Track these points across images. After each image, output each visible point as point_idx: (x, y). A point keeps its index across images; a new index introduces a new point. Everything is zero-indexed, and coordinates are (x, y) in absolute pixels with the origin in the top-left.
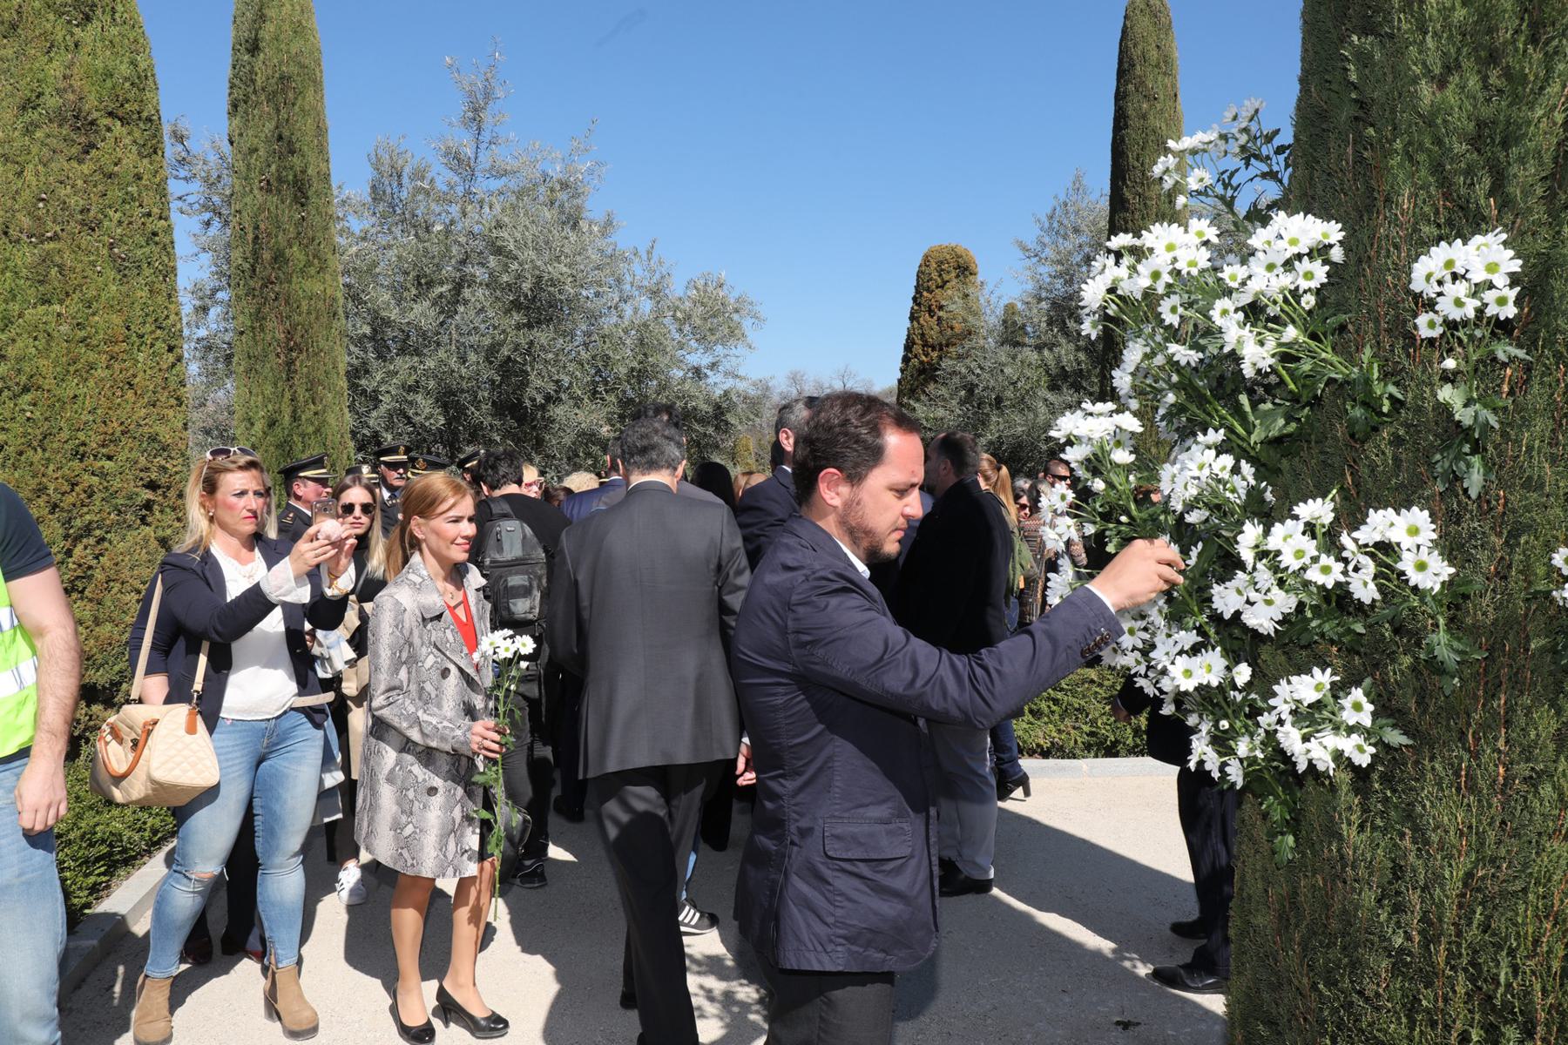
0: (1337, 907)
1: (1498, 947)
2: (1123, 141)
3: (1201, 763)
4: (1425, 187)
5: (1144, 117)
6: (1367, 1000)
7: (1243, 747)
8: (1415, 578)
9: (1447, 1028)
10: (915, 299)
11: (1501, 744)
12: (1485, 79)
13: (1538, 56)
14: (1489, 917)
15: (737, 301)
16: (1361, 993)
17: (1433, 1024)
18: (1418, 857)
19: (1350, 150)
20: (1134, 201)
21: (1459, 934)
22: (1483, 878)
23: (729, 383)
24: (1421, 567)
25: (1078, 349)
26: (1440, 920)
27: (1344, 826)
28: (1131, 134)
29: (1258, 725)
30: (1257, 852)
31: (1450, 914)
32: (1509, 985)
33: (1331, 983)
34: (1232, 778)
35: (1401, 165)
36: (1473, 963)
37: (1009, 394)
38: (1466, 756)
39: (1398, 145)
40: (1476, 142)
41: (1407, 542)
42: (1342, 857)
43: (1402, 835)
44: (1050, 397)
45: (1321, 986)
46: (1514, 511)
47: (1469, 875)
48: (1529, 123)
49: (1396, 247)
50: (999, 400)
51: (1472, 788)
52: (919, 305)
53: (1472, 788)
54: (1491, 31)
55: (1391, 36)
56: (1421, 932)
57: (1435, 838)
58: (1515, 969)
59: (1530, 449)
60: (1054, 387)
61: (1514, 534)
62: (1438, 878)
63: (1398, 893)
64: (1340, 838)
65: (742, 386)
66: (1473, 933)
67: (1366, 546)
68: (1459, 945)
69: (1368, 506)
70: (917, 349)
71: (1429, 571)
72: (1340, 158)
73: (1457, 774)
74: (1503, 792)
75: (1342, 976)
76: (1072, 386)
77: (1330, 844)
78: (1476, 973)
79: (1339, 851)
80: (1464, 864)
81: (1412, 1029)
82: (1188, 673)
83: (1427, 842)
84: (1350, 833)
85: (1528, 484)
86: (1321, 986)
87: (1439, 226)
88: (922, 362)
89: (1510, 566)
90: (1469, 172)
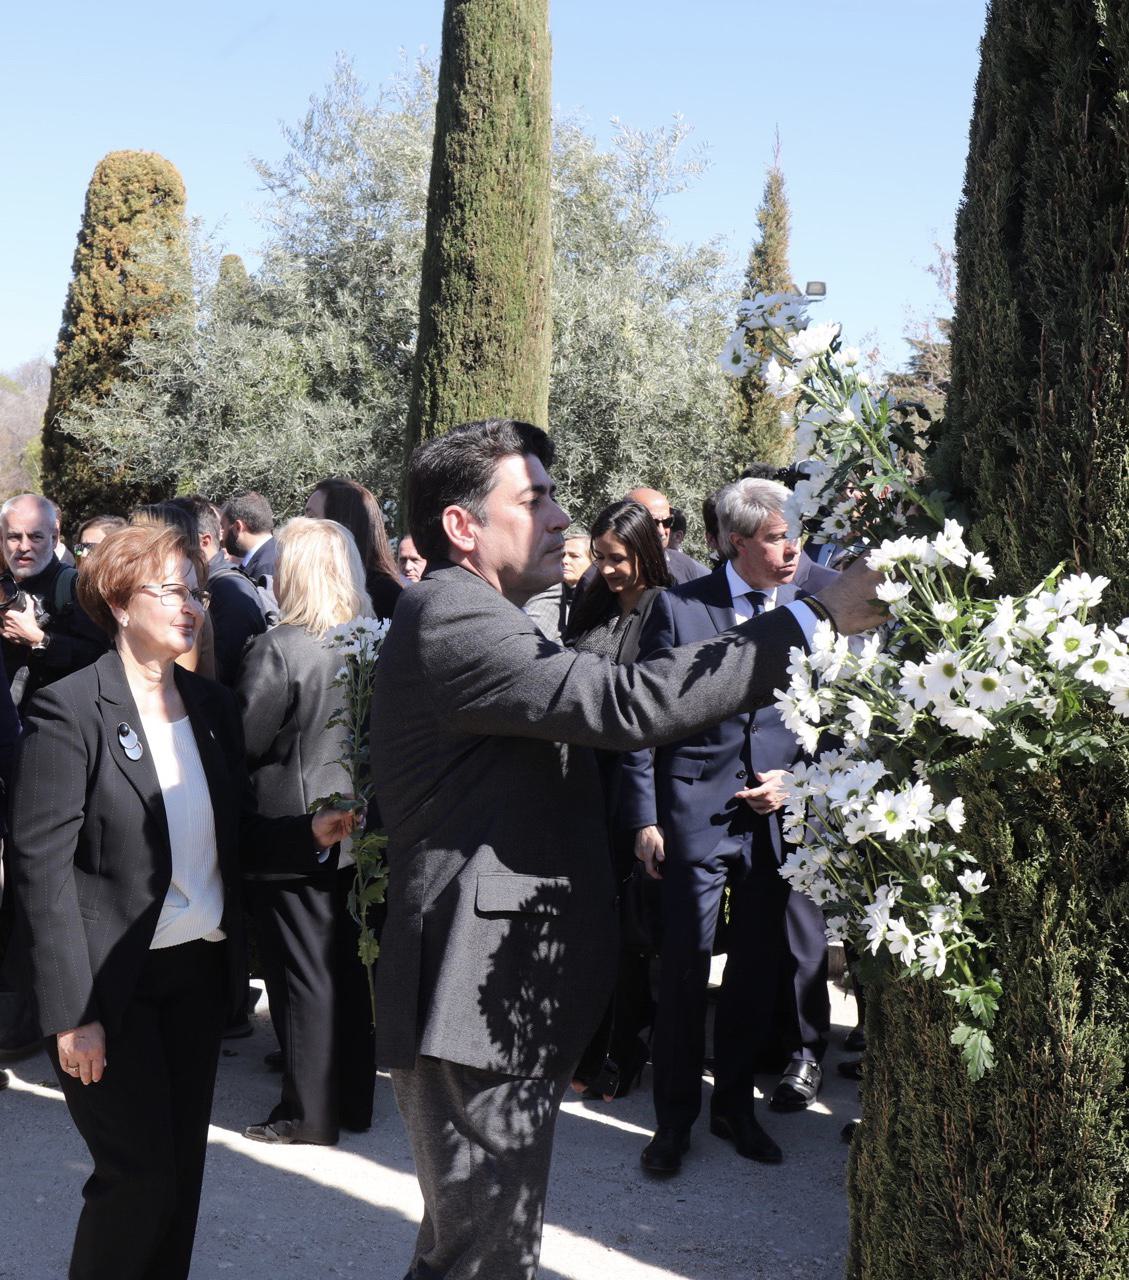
0: (1046, 1126)
2: (462, 20)
3: (884, 945)
6: (1085, 1246)
7: (937, 921)
16: (1078, 1239)
27: (1062, 1017)
29: (959, 888)
30: (921, 1067)
33: (1037, 1230)
34: (929, 961)
42: (1058, 1059)
45: (1026, 1236)
50: (227, 411)
60: (315, 395)
64: (1056, 1039)
76: (345, 394)
77: (1041, 1044)
79: (1053, 1050)
84: (1068, 1027)
86: (1026, 1236)
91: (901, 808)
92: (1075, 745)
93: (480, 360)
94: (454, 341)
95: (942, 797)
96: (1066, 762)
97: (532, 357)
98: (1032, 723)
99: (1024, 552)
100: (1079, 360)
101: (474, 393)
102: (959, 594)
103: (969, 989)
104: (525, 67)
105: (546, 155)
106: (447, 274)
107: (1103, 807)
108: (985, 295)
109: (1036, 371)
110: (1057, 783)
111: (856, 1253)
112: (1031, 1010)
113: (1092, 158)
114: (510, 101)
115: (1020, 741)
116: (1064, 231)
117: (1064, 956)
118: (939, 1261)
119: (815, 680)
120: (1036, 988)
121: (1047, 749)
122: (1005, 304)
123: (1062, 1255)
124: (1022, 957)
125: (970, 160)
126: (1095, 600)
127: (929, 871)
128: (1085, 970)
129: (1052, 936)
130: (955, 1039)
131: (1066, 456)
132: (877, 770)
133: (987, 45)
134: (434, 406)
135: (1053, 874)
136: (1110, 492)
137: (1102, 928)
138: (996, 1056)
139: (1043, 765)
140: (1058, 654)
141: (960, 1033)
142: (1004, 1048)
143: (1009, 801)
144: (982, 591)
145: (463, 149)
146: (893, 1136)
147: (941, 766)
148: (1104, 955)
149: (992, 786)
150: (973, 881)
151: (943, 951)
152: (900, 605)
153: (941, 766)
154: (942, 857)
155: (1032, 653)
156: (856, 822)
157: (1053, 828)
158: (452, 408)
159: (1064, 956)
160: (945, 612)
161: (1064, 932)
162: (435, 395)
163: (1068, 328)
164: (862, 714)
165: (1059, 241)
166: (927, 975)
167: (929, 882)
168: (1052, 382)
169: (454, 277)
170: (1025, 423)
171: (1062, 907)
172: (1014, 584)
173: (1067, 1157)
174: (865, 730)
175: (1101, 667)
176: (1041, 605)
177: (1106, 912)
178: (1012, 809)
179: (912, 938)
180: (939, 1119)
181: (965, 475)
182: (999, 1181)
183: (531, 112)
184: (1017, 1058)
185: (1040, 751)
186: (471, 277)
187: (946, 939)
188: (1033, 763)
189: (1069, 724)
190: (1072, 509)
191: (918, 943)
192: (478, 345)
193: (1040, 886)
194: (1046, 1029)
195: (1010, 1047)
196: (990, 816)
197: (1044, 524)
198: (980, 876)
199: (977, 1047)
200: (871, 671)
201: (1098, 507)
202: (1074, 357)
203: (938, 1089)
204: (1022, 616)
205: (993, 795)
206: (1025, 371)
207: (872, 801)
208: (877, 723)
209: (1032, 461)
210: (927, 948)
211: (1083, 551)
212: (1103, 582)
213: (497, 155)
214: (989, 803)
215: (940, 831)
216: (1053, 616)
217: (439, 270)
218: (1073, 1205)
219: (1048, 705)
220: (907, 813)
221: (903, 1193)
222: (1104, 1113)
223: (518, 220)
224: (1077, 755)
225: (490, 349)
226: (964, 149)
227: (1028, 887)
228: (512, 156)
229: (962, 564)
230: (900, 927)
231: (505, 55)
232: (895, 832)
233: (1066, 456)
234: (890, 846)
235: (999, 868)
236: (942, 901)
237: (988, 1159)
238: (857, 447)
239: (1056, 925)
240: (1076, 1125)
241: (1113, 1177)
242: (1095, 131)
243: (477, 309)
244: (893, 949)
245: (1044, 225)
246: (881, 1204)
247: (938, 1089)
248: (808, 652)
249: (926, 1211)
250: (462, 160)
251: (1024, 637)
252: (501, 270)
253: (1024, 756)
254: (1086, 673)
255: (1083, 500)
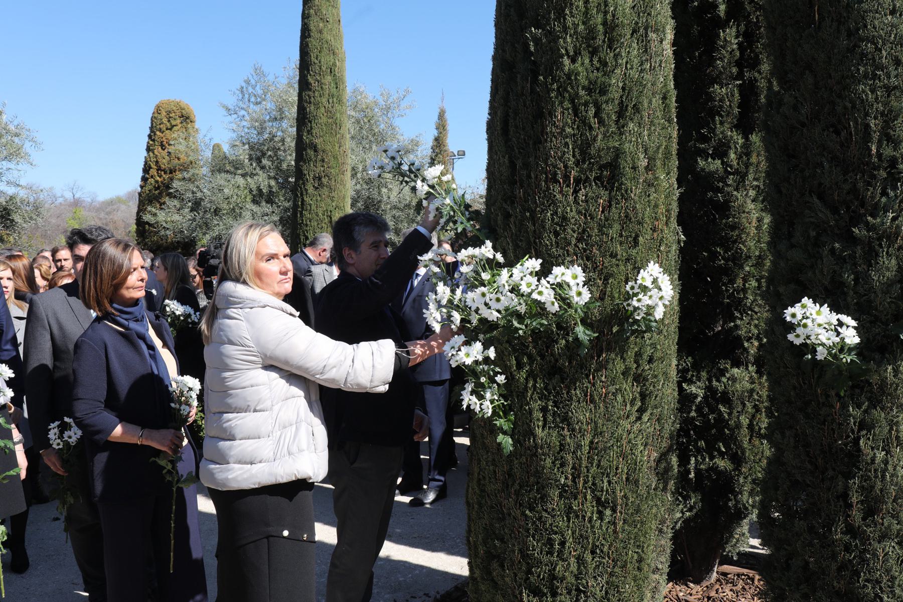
1: (603, 474)
2: (308, 45)
3: (469, 406)
4: (568, 109)
5: (321, 32)
7: (488, 395)
8: (576, 299)
9: (584, 517)
10: (150, 136)
11: (603, 379)
12: (591, 61)
13: (612, 55)
14: (599, 461)
15: (17, 127)
16: (546, 511)
17: (577, 517)
18: (570, 438)
19: (529, 85)
20: (315, 85)
21: (588, 471)
22: (597, 443)
23: (11, 191)
24: (579, 294)
25: (270, 178)
26: (580, 466)
28: (313, 42)
31: (584, 463)
32: (607, 490)
35: (556, 97)
36: (594, 484)
37: (225, 206)
38: (589, 386)
39: (555, 86)
40: (589, 90)
41: (572, 283)
43: (563, 429)
44: (255, 208)
45: (527, 512)
46: (606, 267)
47: (591, 442)
48: (610, 85)
49: (555, 137)
51: (592, 401)
52: (154, 140)
53: (592, 401)
54: (594, 38)
55: (550, 32)
56: (572, 475)
57: (577, 427)
58: (609, 482)
59: (612, 238)
60: (255, 202)
61: (606, 279)
62: (579, 446)
63: (562, 458)
64: (535, 436)
65: (22, 194)
66: (594, 469)
67: (553, 284)
68: (588, 477)
69: (553, 265)
70: (153, 172)
71: (581, 296)
72: (523, 88)
73: (586, 395)
74: (604, 401)
75: (537, 504)
76: (267, 202)
77: (529, 439)
78: (594, 488)
79: (534, 441)
80: (588, 438)
81: (569, 521)
82: (468, 355)
83: (574, 430)
84: (539, 432)
85: (611, 256)
86: (527, 512)
87: (573, 129)
88: (157, 182)
89: (605, 294)
90: (586, 104)
91: (471, 352)
92: (534, 324)
93: (321, 185)
94: (310, 178)
95: (486, 347)
96: (533, 331)
97: (343, 183)
98: (520, 317)
99: (515, 250)
100: (531, 178)
101: (319, 198)
102: (491, 269)
103: (502, 420)
104: (334, 65)
105: (345, 101)
106: (306, 150)
107: (547, 347)
108: (496, 154)
109: (516, 183)
110: (530, 339)
111: (469, 526)
112: (525, 426)
113: (532, 101)
114: (329, 78)
115: (516, 324)
116: (524, 129)
117: (536, 405)
118: (497, 525)
119: (439, 306)
120: (527, 418)
121: (526, 326)
122: (504, 157)
123: (541, 517)
124: (521, 407)
125: (490, 102)
126: (538, 268)
127: (485, 376)
128: (544, 410)
129: (531, 398)
130: (498, 441)
131: (528, 214)
132: (462, 338)
133: (495, 58)
134: (303, 204)
135: (531, 374)
136: (544, 227)
137: (550, 393)
138: (514, 445)
139: (525, 333)
140: (524, 289)
141: (500, 438)
142: (516, 442)
143: (513, 347)
144: (500, 266)
145: (310, 98)
146: (479, 480)
147: (488, 336)
148: (551, 403)
149: (507, 342)
150: (501, 379)
151: (490, 407)
152: (470, 274)
153: (488, 336)
154: (488, 370)
155: (515, 290)
156: (454, 359)
157: (530, 357)
158: (310, 205)
159: (536, 405)
160: (485, 276)
161: (536, 396)
162: (303, 200)
163: (526, 165)
164: (457, 317)
165: (522, 132)
166: (486, 416)
167: (483, 380)
168: (522, 186)
169: (309, 151)
170: (513, 203)
171: (534, 386)
172: (510, 264)
173: (540, 481)
174: (458, 322)
175: (540, 293)
176: (517, 271)
177: (550, 387)
178: (515, 350)
179: (478, 403)
180: (495, 472)
181: (492, 223)
182: (517, 493)
183: (338, 82)
184: (521, 445)
185: (524, 327)
186: (316, 151)
187: (492, 402)
188: (521, 332)
189: (532, 316)
190: (531, 234)
191: (481, 404)
192: (320, 178)
193: (526, 379)
194: (532, 433)
195: (519, 442)
196: (506, 353)
197: (521, 241)
198: (503, 377)
199: (506, 442)
200: (460, 300)
201: (540, 233)
202: (529, 176)
203: (494, 460)
204: (511, 276)
205: (508, 345)
206: (512, 183)
207: (460, 350)
208: (462, 320)
209: (516, 217)
210: (484, 405)
211: (536, 250)
212: (540, 261)
213: (324, 100)
214: (506, 349)
215: (487, 360)
216: (522, 275)
217: (301, 147)
218: (544, 498)
219: (522, 309)
220: (471, 354)
221: (483, 502)
222: (553, 463)
223: (334, 127)
224: (536, 328)
225: (325, 181)
226: (488, 97)
227: (522, 380)
228: (331, 101)
229: (492, 257)
230: (474, 399)
231: (326, 60)
232: (469, 361)
233: (528, 214)
234: (467, 366)
235: (511, 373)
236: (490, 388)
237: (513, 484)
238: (452, 213)
239: (533, 393)
240: (544, 468)
241: (557, 486)
242: (533, 91)
243: (319, 164)
244: (472, 407)
245: (516, 127)
246: (476, 506)
247: (494, 460)
248: (436, 294)
249: (493, 507)
250: (310, 103)
251: (513, 283)
252: (328, 148)
253: (517, 329)
254: (535, 296)
255: (535, 231)
